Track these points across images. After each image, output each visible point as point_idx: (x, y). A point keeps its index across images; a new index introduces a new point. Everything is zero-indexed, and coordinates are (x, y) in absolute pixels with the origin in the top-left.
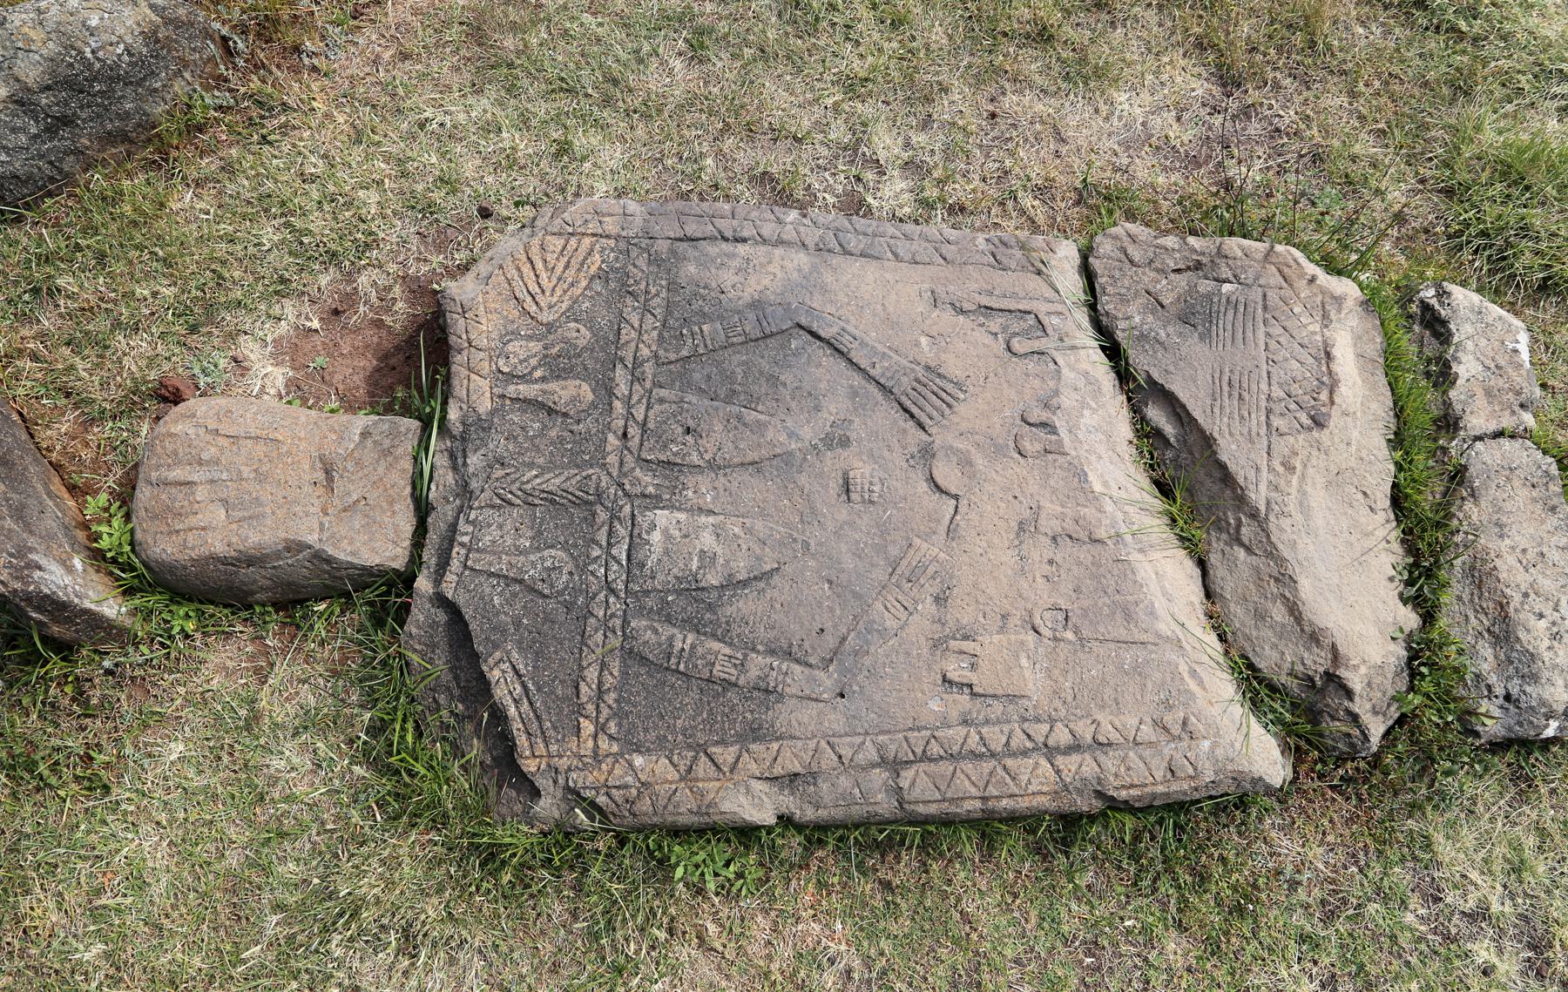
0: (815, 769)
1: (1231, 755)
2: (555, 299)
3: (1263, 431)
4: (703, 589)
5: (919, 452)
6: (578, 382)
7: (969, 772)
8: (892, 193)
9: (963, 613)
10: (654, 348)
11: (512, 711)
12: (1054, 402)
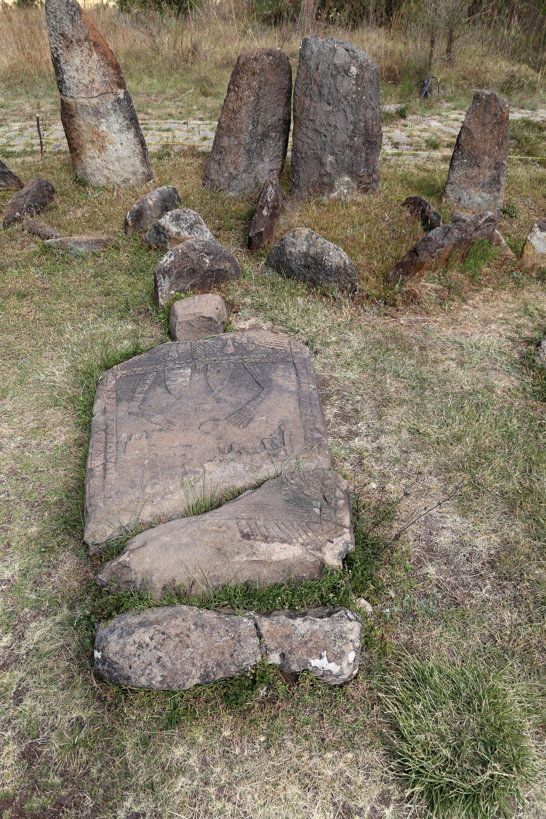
9: (155, 436)
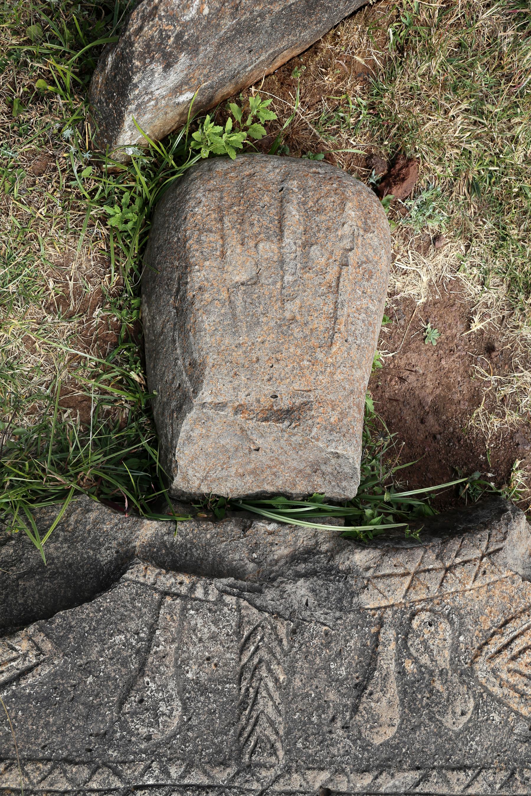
6: (397, 722)
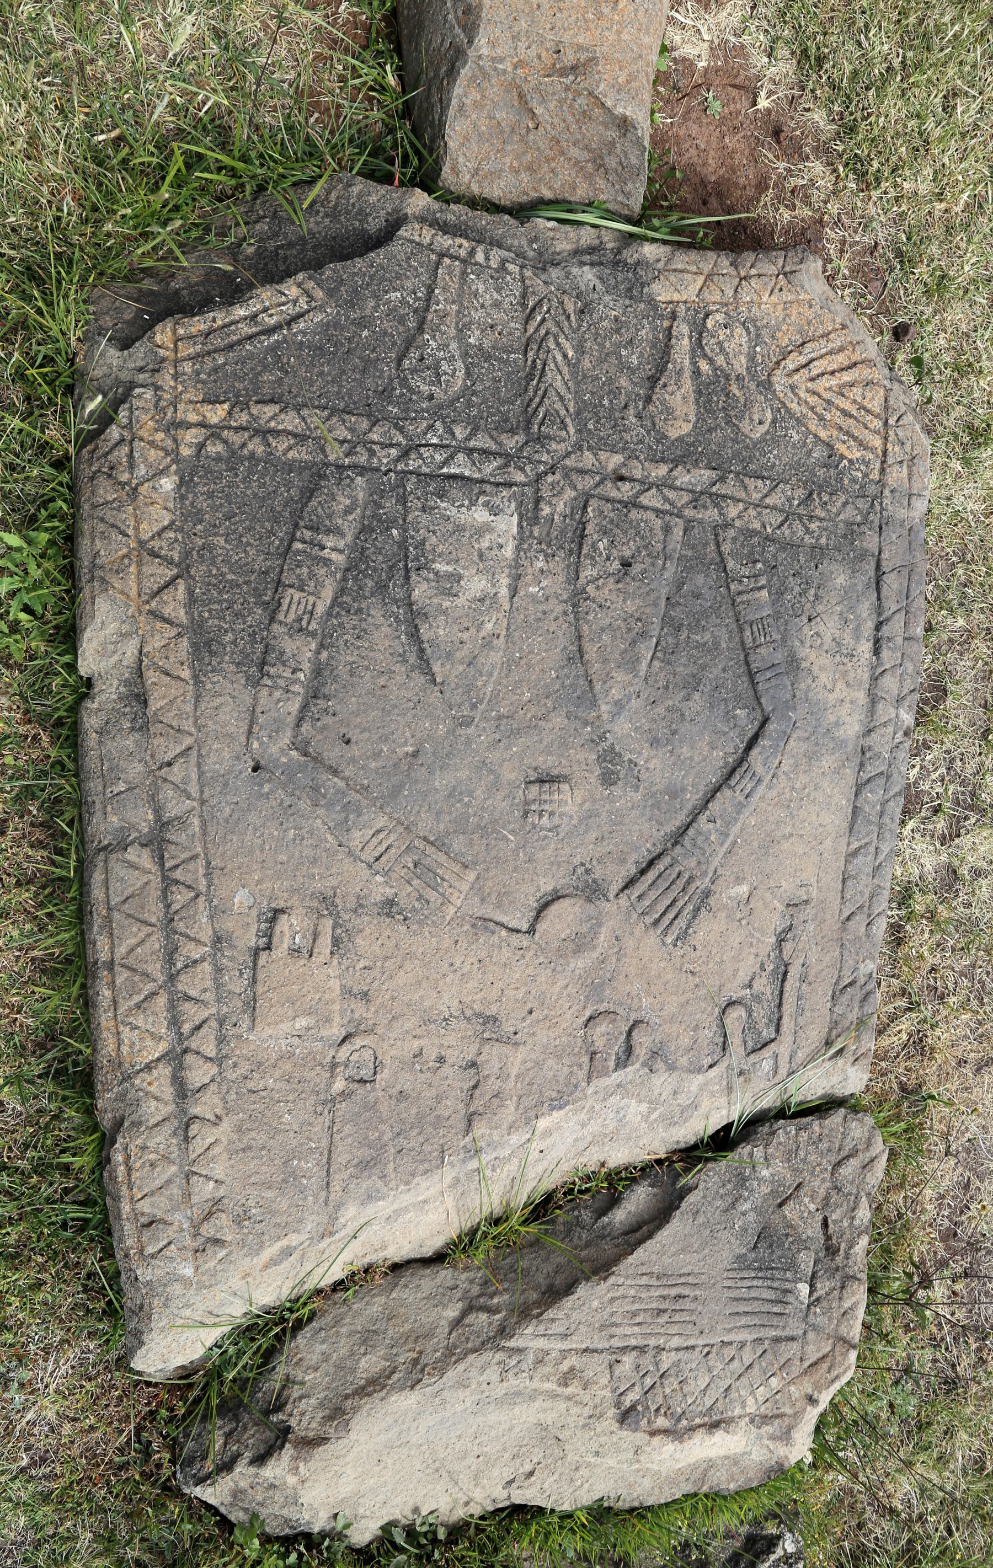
0: (152, 730)
1: (173, 1304)
2: (802, 394)
3: (616, 1343)
4: (407, 578)
5: (594, 881)
6: (693, 418)
7: (148, 945)
8: (918, 853)
10: (738, 523)
11: (240, 312)
12: (659, 1065)
